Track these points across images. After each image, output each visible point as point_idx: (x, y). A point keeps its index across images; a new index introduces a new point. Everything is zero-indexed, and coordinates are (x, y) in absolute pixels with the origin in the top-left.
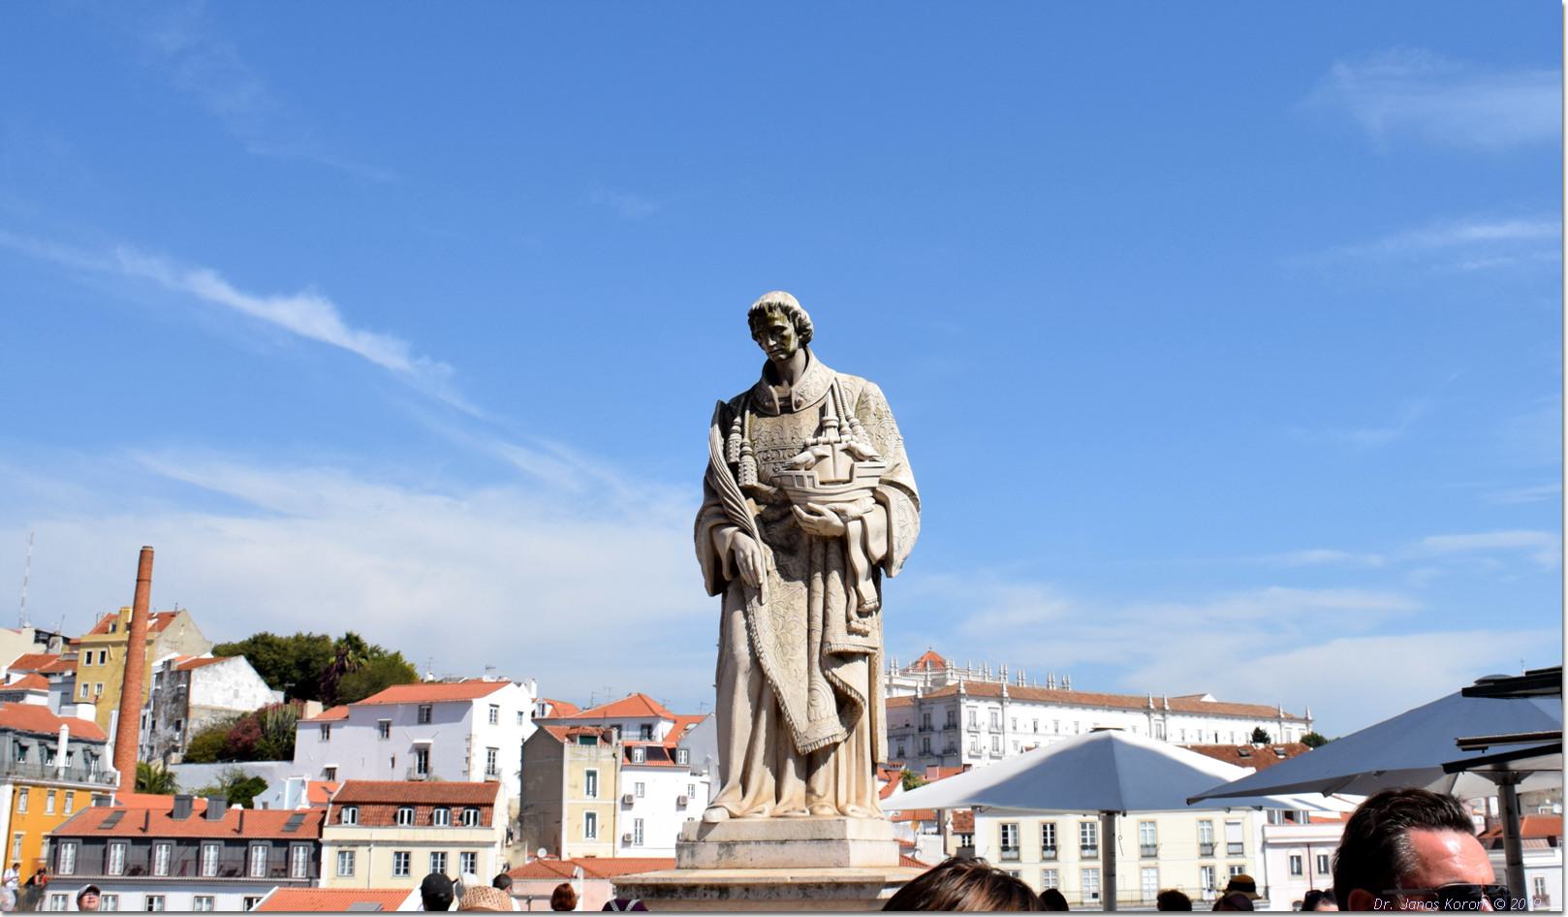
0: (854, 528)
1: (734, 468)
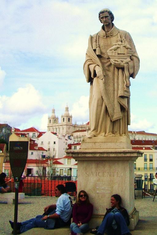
0: (125, 65)
1: (95, 50)
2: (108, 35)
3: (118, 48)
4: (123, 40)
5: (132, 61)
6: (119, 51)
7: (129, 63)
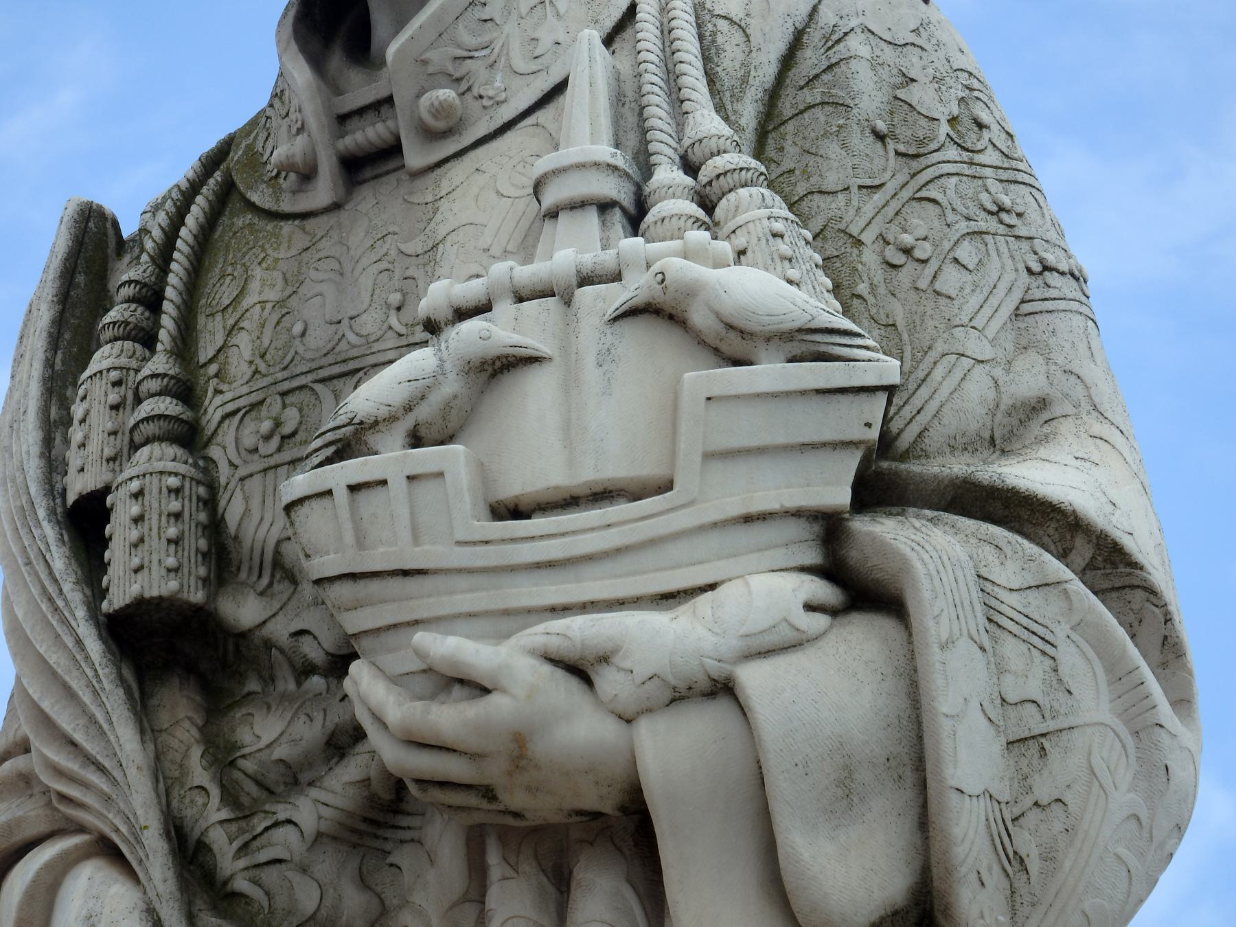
2: (369, 133)
3: (502, 367)
4: (667, 174)
5: (864, 637)
6: (534, 440)
7: (754, 679)
